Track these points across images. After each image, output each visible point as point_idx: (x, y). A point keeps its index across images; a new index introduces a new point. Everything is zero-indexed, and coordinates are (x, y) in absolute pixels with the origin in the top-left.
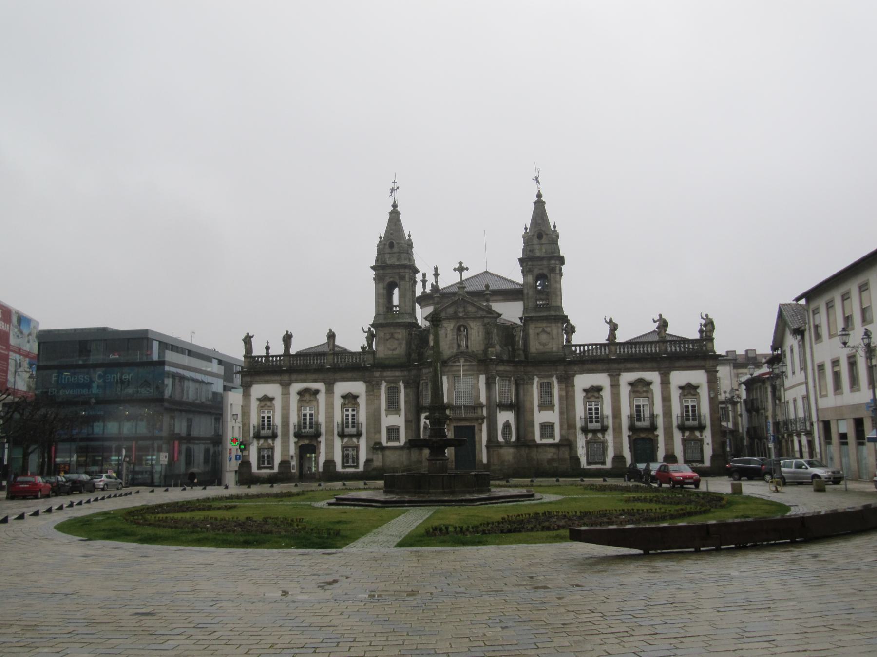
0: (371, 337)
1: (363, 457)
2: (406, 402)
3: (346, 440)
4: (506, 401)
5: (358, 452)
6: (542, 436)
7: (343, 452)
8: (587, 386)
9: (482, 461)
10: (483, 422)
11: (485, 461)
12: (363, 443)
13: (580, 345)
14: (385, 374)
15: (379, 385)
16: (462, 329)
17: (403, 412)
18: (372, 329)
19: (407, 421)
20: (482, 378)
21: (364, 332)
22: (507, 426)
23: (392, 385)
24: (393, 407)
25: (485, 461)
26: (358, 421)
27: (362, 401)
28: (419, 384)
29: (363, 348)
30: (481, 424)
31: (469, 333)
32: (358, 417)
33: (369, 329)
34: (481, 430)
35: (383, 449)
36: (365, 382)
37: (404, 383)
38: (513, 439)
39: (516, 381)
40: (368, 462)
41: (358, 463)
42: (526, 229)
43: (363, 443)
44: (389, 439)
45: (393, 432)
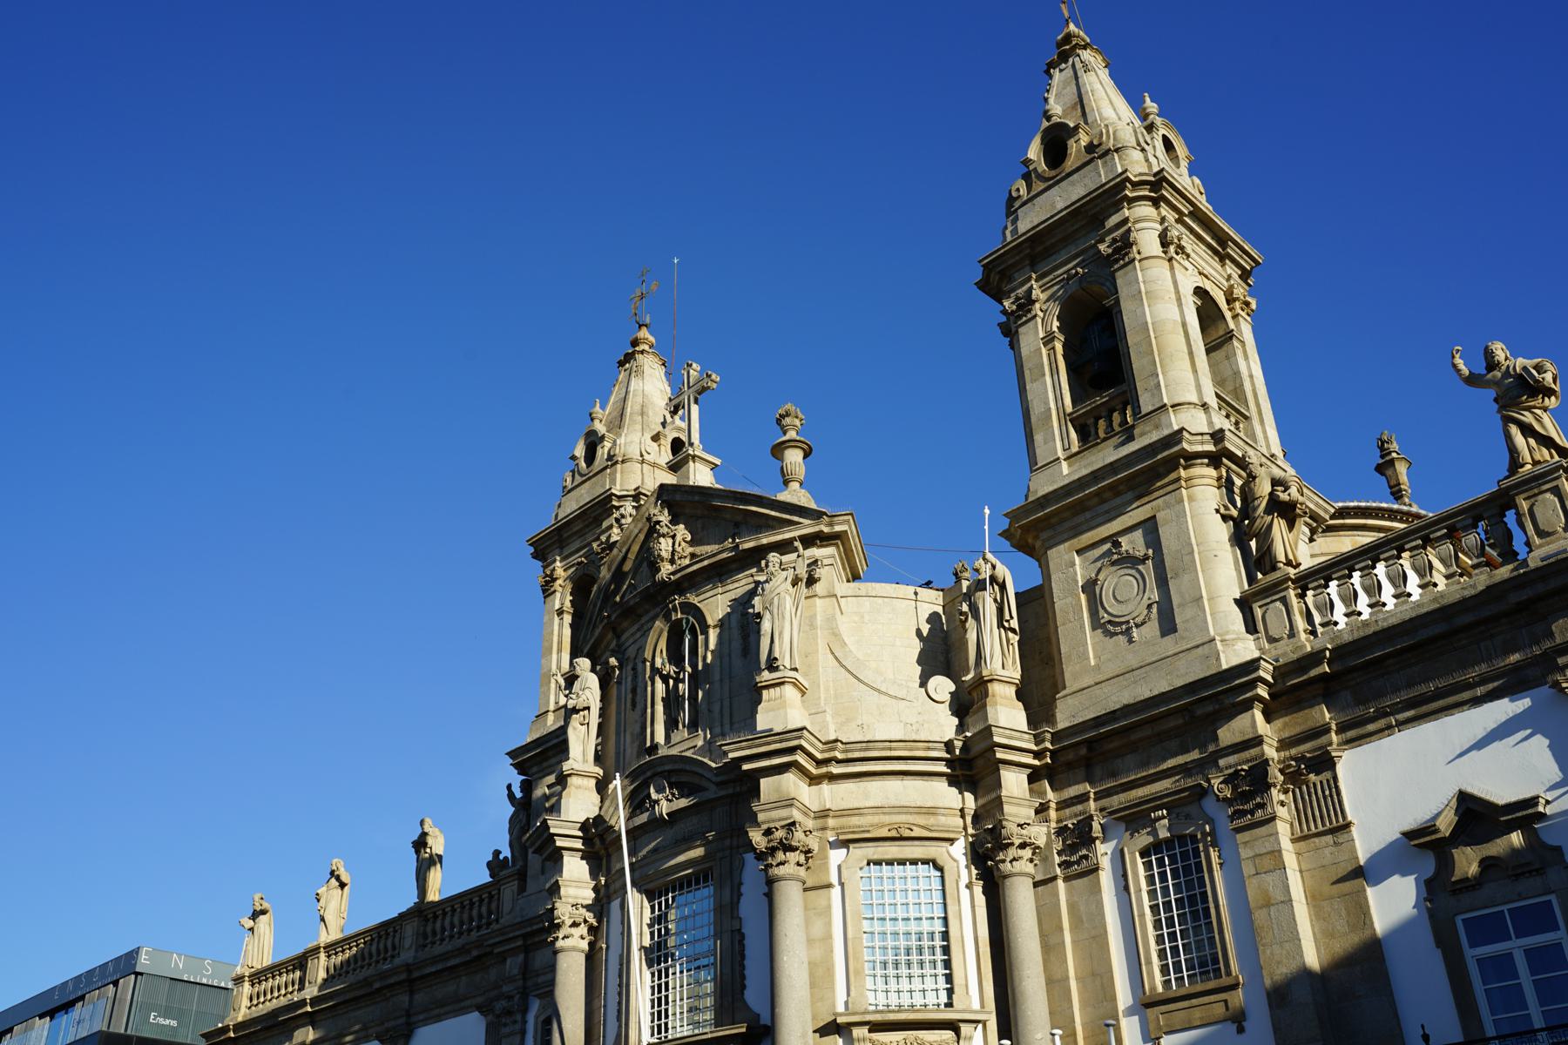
8: (1430, 802)
29: (496, 865)
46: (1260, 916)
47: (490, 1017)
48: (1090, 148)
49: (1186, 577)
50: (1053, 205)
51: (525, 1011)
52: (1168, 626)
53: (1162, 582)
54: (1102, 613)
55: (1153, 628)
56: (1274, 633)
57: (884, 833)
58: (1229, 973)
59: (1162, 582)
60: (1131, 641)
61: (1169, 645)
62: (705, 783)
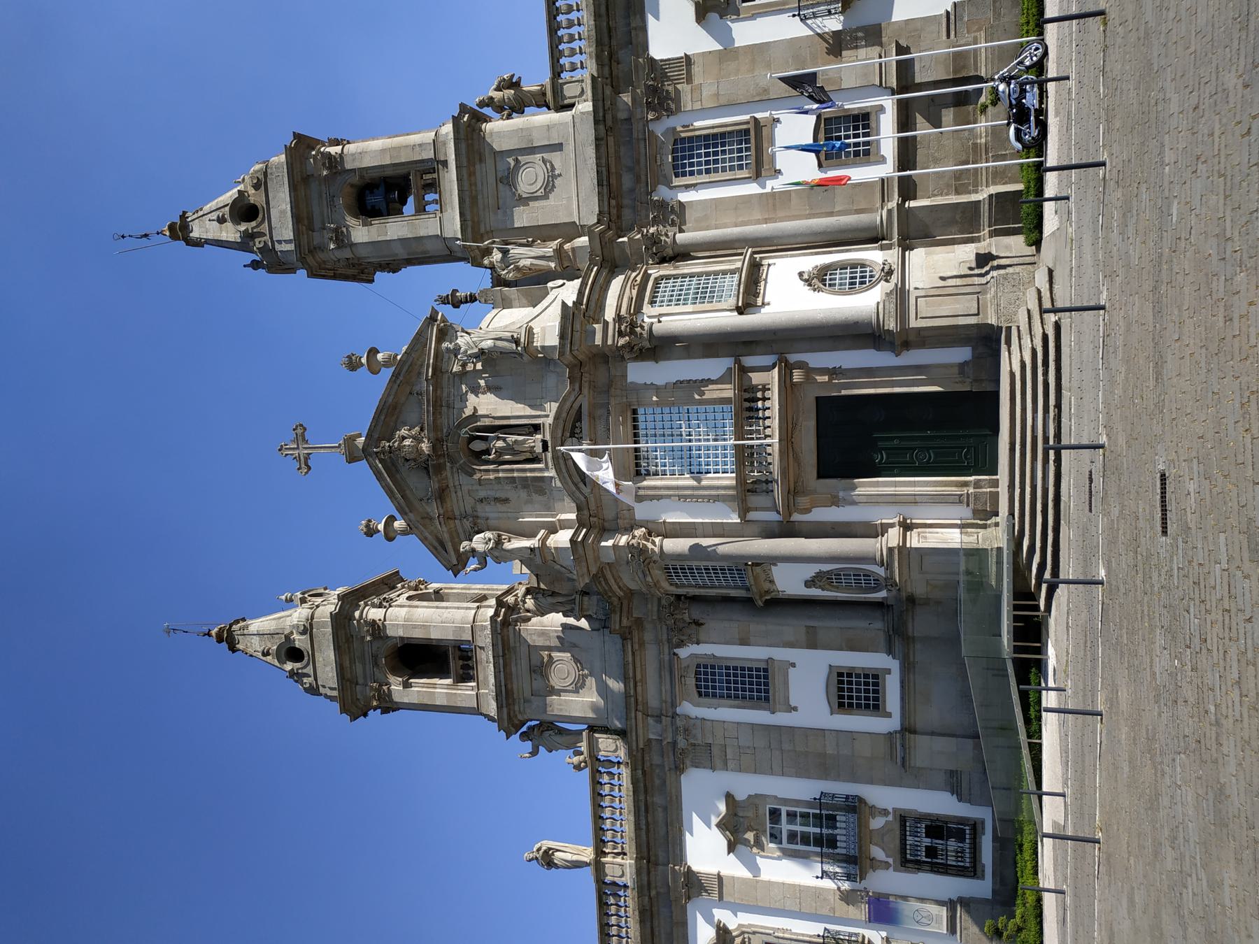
0: (547, 733)
1: (940, 803)
2: (744, 642)
3: (877, 852)
4: (731, 287)
5: (920, 818)
6: (866, 154)
7: (917, 866)
9: (962, 366)
10: (802, 365)
11: (962, 354)
12: (890, 798)
13: (555, 55)
14: (653, 702)
15: (689, 727)
16: (478, 446)
17: (781, 654)
18: (524, 729)
19: (812, 645)
20: (639, 373)
21: (534, 753)
22: (819, 279)
23: (691, 681)
24: (756, 685)
25: (962, 354)
26: (809, 804)
27: (746, 785)
28: (678, 597)
30: (809, 371)
31: (487, 422)
32: (797, 803)
33: (525, 737)
34: (834, 372)
35: (908, 729)
36: (679, 769)
37: (681, 644)
38: (874, 256)
39: (663, 260)
40: (955, 784)
41: (962, 821)
42: (255, 265)
43: (890, 798)
44: (874, 705)
45: (853, 692)
46: (723, 101)
47: (688, 762)
48: (256, 187)
49: (535, 135)
50: (283, 212)
51: (687, 717)
52: (558, 147)
53: (532, 150)
54: (539, 194)
55: (555, 158)
56: (579, 90)
57: (634, 292)
58: (747, 123)
59: (532, 150)
60: (560, 175)
61: (569, 148)
62: (576, 406)
